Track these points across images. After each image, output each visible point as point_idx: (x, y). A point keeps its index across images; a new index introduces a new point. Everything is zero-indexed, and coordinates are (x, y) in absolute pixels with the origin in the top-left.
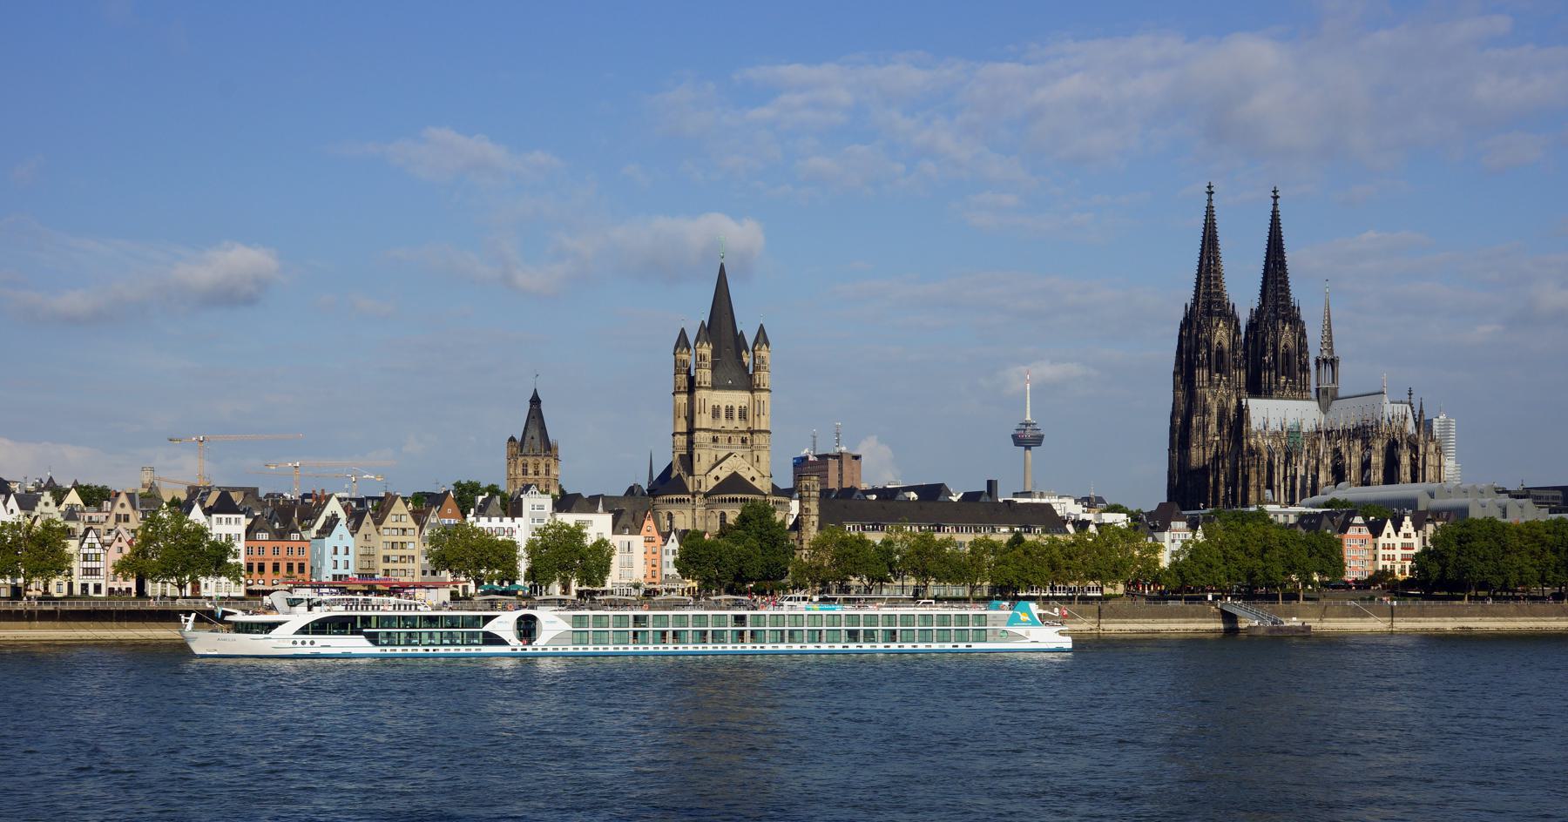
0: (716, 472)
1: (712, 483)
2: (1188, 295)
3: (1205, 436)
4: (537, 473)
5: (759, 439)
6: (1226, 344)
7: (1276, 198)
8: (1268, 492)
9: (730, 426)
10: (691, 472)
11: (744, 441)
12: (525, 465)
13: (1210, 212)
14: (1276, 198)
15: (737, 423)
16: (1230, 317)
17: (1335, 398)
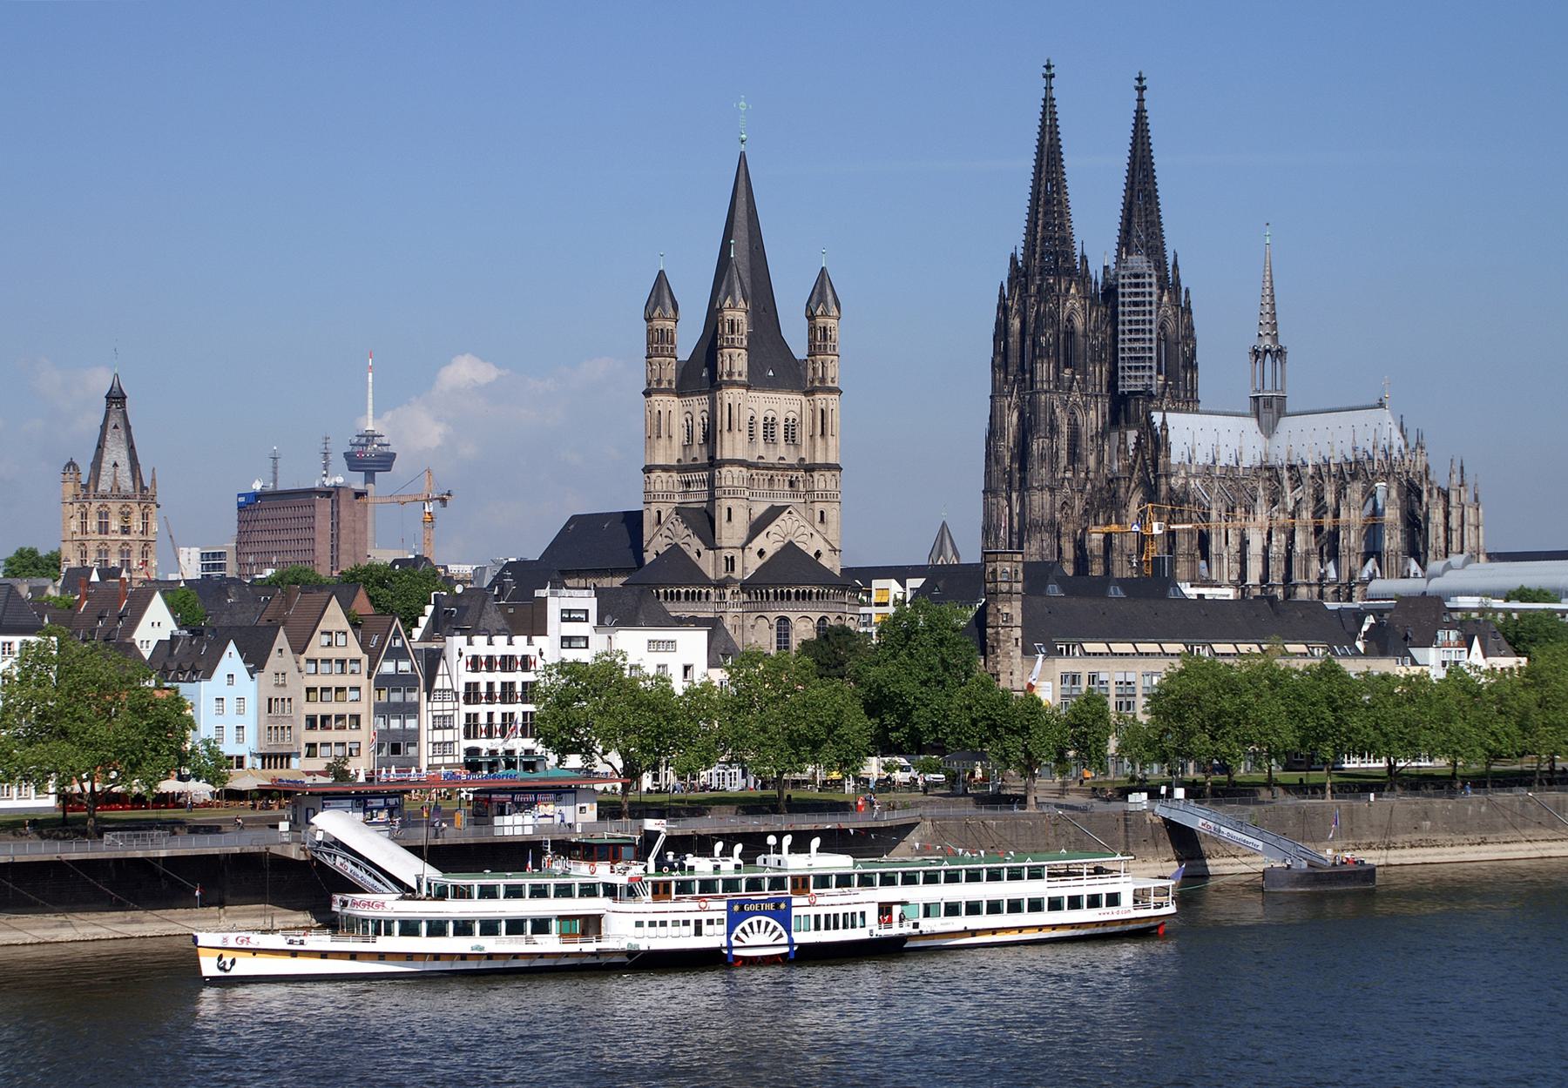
0: (760, 542)
1: (749, 564)
2: (1013, 238)
3: (1053, 471)
4: (126, 530)
5: (821, 481)
6: (1079, 323)
7: (1141, 89)
8: (1203, 563)
9: (772, 459)
10: (711, 542)
11: (791, 484)
12: (103, 514)
13: (1049, 105)
14: (1141, 89)
15: (782, 452)
16: (1084, 278)
17: (1282, 413)
